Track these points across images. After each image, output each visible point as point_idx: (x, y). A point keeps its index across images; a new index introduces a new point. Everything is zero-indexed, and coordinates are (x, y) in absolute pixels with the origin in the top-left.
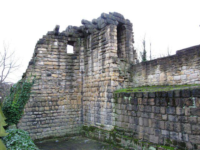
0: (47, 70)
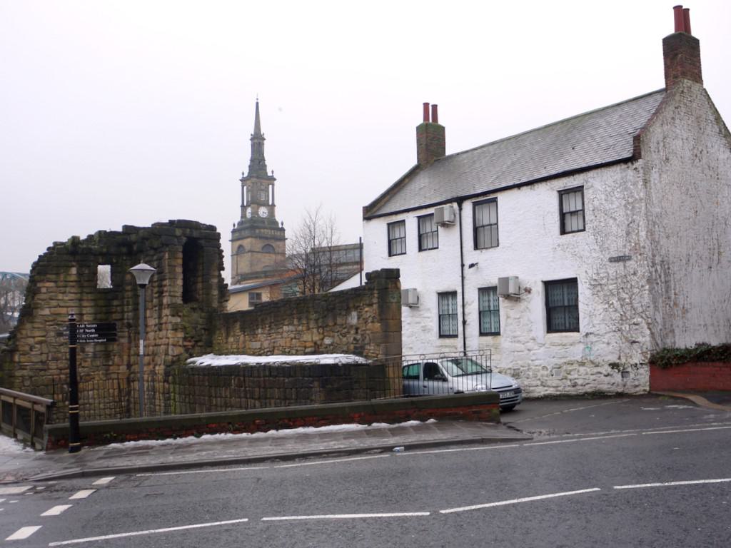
0: (57, 325)
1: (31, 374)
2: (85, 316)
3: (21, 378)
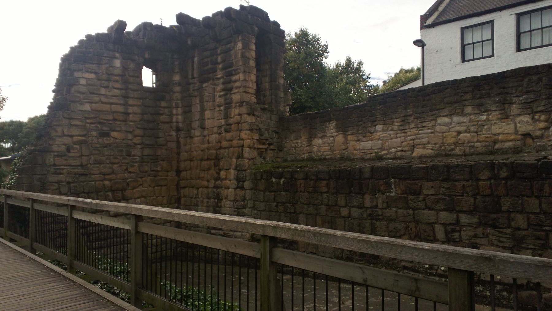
0: (100, 123)
1: (69, 179)
2: (131, 116)
3: (56, 184)
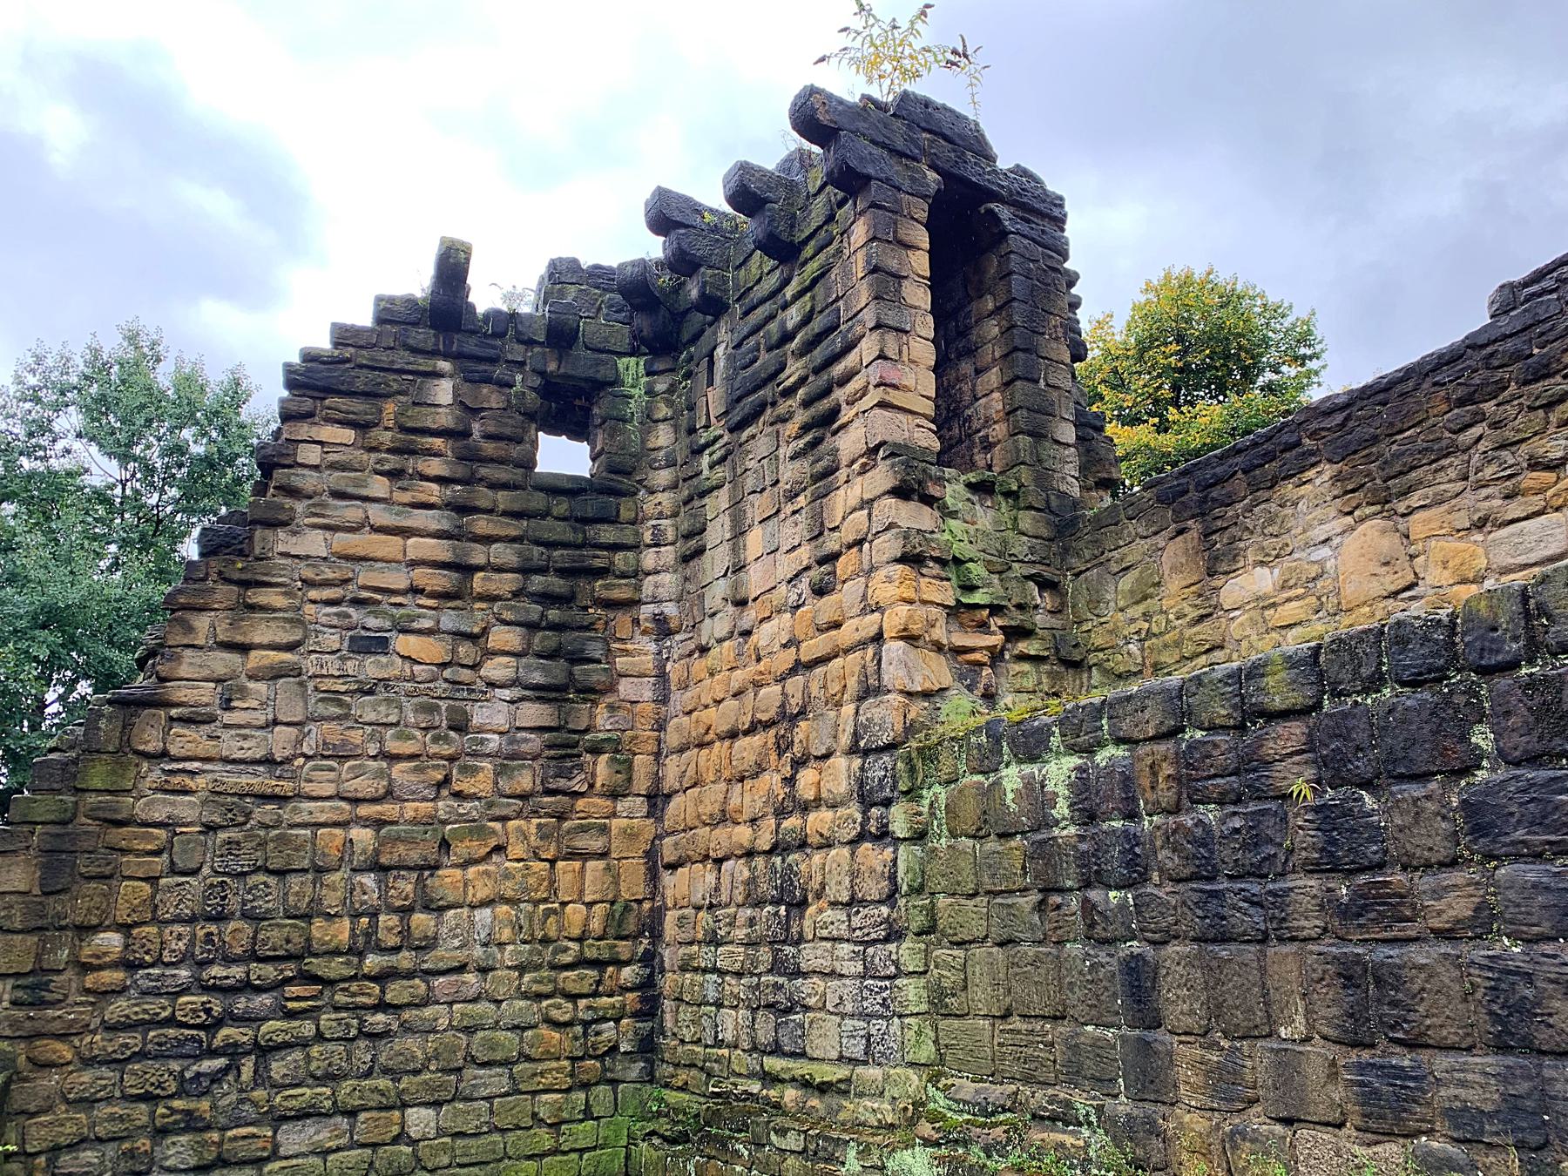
0: (357, 602)
